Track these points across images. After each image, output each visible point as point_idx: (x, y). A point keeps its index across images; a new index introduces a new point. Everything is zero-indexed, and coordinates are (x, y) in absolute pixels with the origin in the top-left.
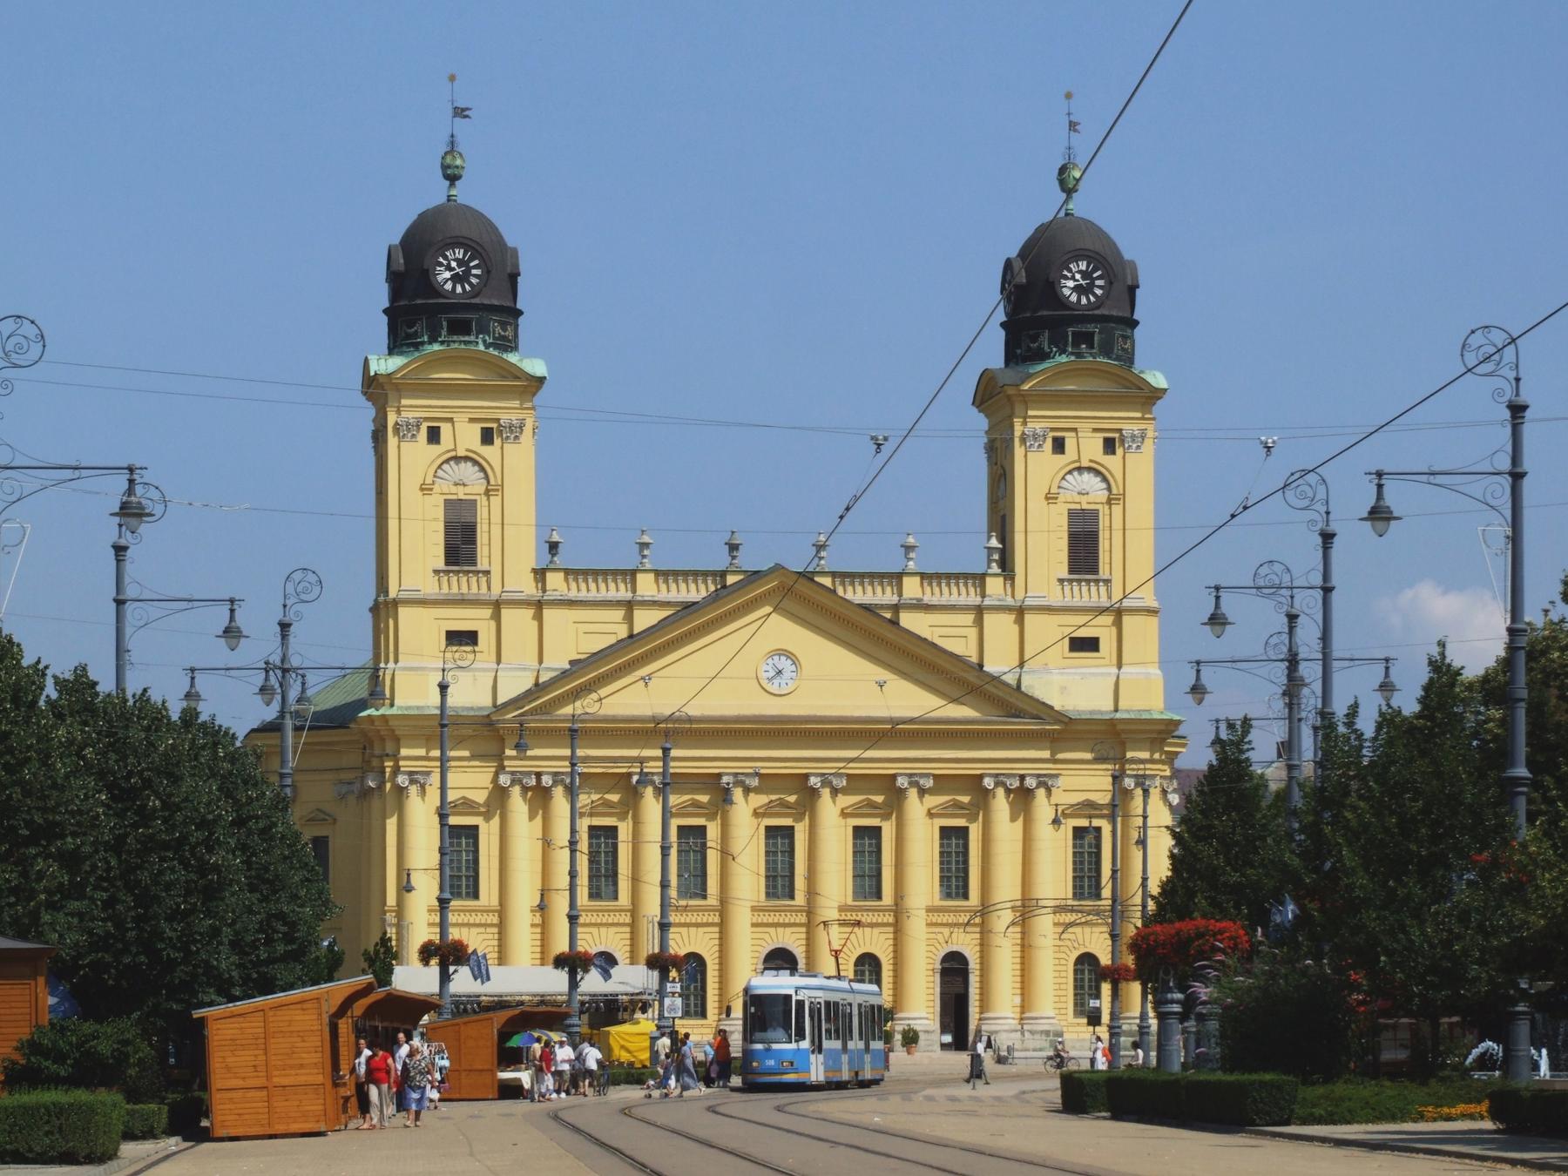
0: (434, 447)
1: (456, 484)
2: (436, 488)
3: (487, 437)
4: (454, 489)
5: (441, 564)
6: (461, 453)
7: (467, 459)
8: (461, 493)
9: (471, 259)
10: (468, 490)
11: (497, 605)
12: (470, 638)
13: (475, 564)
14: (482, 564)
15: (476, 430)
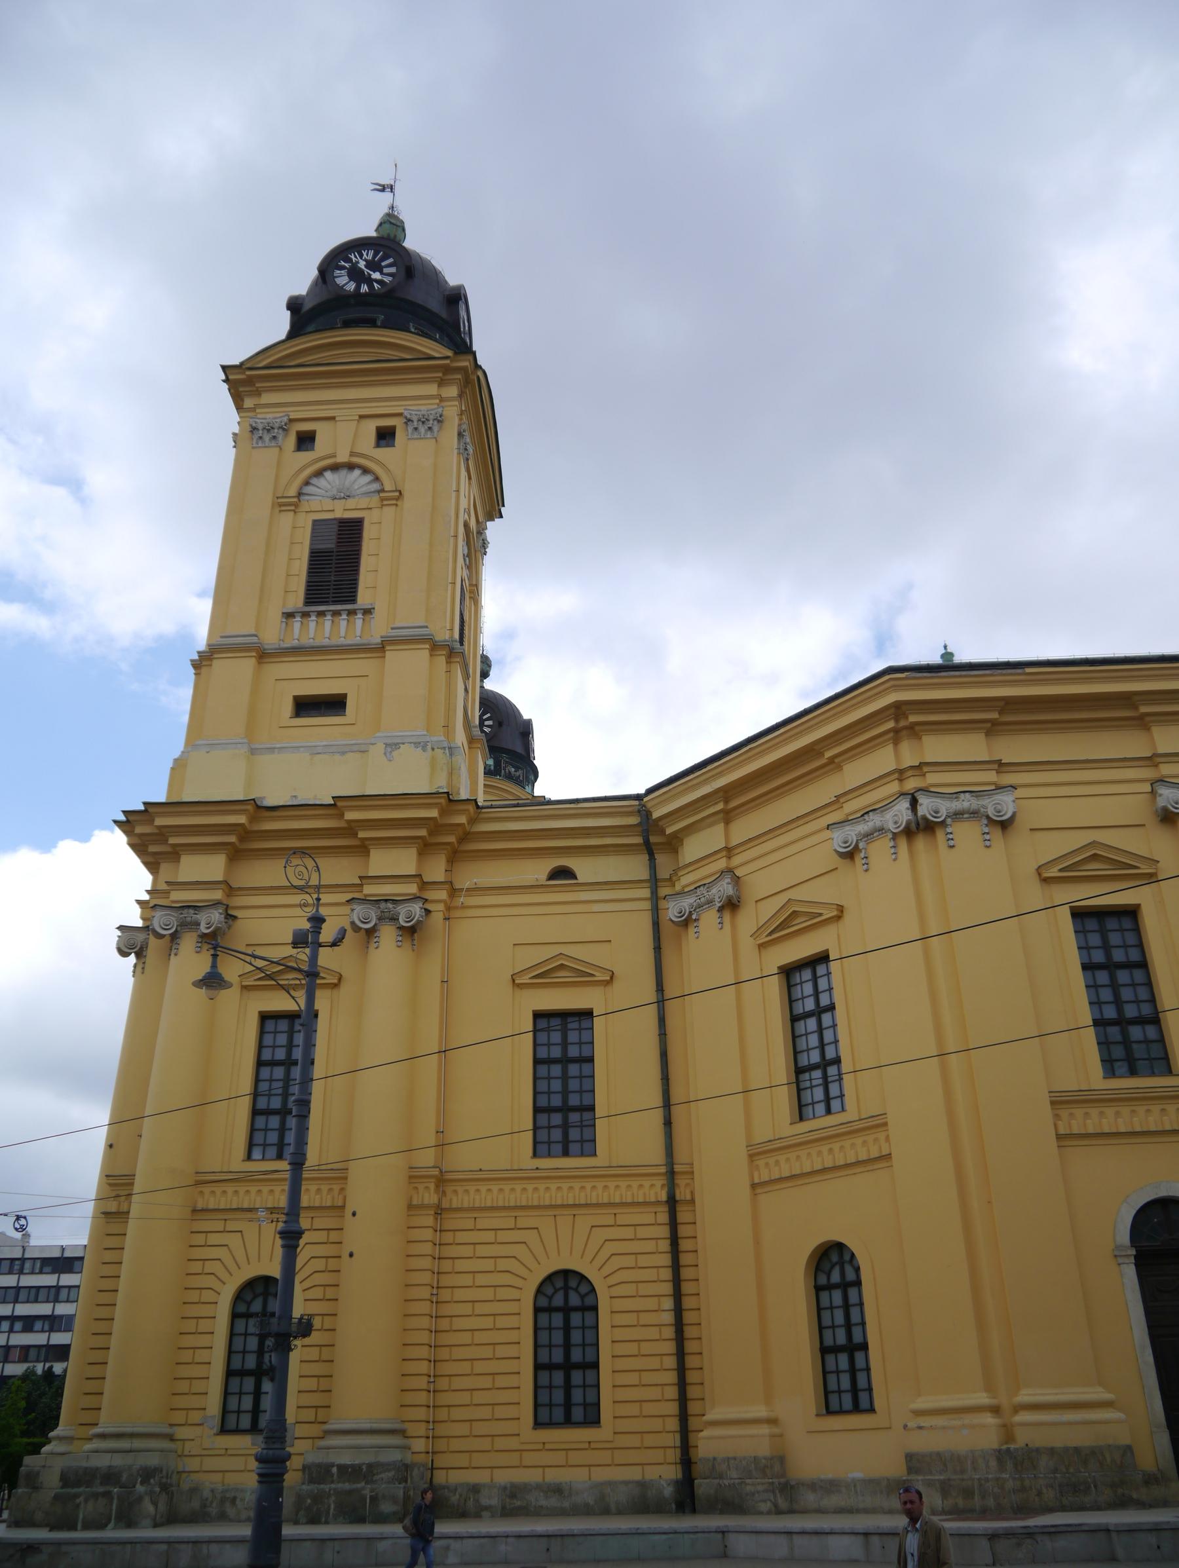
0: (305, 456)
1: (334, 498)
2: (305, 506)
3: (385, 436)
4: (328, 504)
5: (297, 600)
6: (343, 457)
7: (351, 467)
8: (341, 511)
9: (383, 259)
10: (351, 503)
11: (380, 649)
12: (334, 704)
13: (352, 599)
14: (364, 597)
15: (370, 429)
